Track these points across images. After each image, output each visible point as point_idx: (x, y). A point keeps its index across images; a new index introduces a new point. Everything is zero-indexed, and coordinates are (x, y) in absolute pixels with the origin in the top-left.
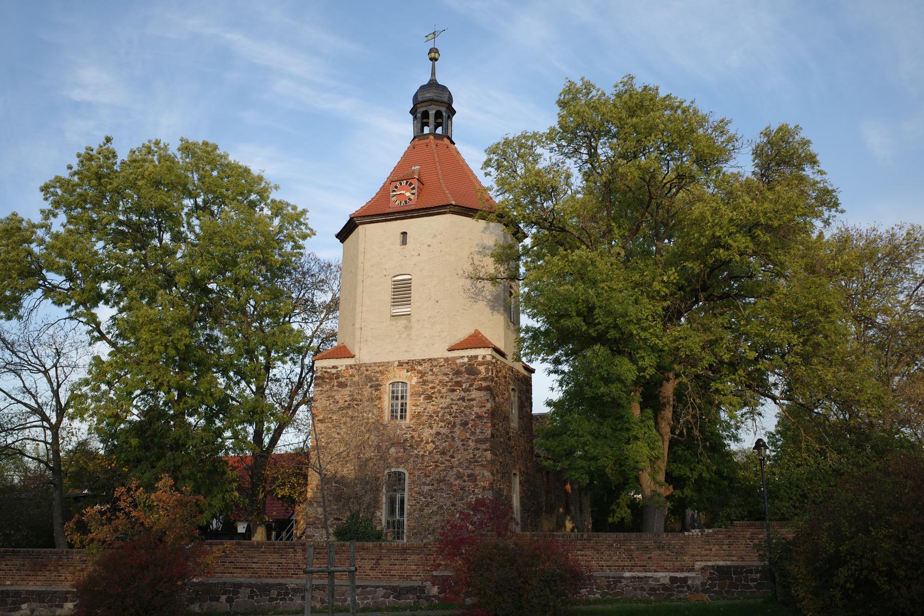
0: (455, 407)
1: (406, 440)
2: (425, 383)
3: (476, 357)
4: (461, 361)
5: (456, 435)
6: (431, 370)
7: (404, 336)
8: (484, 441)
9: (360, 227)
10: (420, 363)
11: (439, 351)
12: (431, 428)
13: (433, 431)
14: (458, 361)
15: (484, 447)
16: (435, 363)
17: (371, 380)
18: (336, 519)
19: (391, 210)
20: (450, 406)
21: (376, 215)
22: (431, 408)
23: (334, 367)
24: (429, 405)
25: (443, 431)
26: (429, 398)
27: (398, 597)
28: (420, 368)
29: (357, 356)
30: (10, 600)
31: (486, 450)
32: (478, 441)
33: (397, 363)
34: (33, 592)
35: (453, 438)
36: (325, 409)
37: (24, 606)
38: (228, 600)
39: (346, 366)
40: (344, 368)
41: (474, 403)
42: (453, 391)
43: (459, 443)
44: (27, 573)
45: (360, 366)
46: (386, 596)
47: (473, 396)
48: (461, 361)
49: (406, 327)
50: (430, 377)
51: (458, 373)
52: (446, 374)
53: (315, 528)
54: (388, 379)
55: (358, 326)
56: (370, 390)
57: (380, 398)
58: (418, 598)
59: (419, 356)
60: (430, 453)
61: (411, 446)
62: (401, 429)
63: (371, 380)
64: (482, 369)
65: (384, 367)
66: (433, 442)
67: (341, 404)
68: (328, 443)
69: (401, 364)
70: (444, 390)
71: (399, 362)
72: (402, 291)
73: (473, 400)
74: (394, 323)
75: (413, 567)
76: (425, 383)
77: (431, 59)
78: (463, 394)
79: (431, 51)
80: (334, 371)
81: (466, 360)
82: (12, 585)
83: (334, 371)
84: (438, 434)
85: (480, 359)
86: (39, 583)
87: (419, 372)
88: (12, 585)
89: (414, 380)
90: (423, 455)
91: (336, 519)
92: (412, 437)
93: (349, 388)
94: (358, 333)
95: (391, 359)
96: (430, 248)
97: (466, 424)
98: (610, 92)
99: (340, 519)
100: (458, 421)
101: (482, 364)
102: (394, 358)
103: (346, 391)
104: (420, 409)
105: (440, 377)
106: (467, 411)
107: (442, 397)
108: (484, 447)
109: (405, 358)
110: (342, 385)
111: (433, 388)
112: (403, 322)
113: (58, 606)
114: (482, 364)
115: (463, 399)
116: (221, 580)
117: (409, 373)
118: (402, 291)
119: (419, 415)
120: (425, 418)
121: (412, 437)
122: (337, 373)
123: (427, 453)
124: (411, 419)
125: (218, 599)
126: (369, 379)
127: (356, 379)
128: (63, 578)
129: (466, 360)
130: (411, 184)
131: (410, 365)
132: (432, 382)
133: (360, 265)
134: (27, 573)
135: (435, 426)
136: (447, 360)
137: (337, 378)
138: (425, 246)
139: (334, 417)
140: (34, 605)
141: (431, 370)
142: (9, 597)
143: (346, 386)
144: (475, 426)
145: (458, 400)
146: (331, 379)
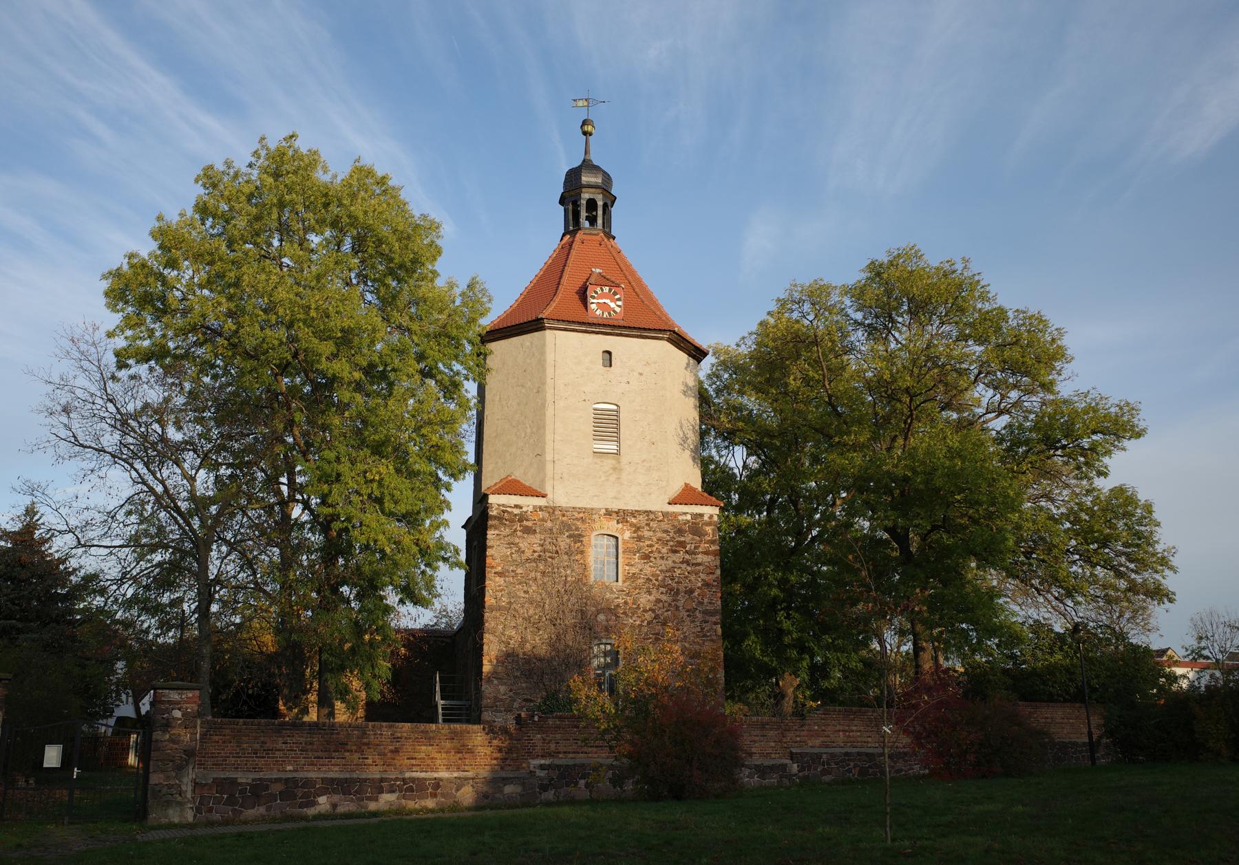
0: (678, 571)
1: (618, 606)
2: (640, 539)
3: (701, 515)
4: (684, 517)
5: (680, 604)
6: (648, 525)
7: (612, 478)
8: (712, 614)
9: (548, 332)
10: (634, 514)
11: (658, 503)
12: (650, 594)
13: (652, 598)
14: (680, 518)
15: (714, 619)
16: (652, 516)
17: (569, 529)
18: (526, 700)
19: (590, 321)
20: (672, 570)
21: (604, 325)
22: (648, 570)
23: (516, 506)
24: (647, 567)
25: (664, 598)
26: (646, 557)
27: (762, 777)
28: (633, 520)
29: (550, 496)
30: (299, 792)
31: (715, 624)
32: (705, 612)
33: (603, 511)
34: (332, 780)
35: (677, 608)
36: (504, 558)
37: (322, 800)
38: (587, 785)
39: (534, 507)
40: (531, 509)
41: (701, 568)
42: (676, 552)
43: (684, 614)
44: (316, 754)
45: (554, 509)
46: (750, 776)
47: (699, 560)
48: (684, 517)
49: (614, 469)
50: (647, 534)
51: (680, 532)
52: (666, 531)
53: (496, 711)
54: (592, 530)
55: (549, 457)
56: (568, 541)
57: (582, 552)
58: (781, 777)
59: (631, 507)
60: (649, 623)
61: (624, 613)
62: (612, 592)
63: (569, 529)
64: (709, 529)
65: (586, 515)
66: (653, 611)
67: (528, 554)
68: (510, 603)
69: (609, 513)
70: (664, 551)
71: (607, 510)
72: (608, 424)
73: (699, 564)
74: (598, 461)
75: (773, 744)
76: (640, 539)
77: (585, 133)
78: (687, 557)
79: (585, 123)
80: (516, 511)
81: (689, 517)
82: (295, 771)
83: (516, 511)
84: (658, 601)
85: (706, 518)
86: (337, 768)
87: (632, 525)
88: (295, 771)
89: (627, 535)
90: (640, 626)
91: (526, 700)
92: (626, 603)
93: (538, 536)
94: (549, 466)
95: (595, 504)
96: (642, 378)
97: (691, 591)
98: (935, 263)
99: (531, 701)
100: (682, 588)
101: (709, 524)
102: (599, 504)
103: (536, 539)
104: (634, 570)
105: (659, 535)
106: (693, 578)
107: (662, 558)
108: (714, 619)
109: (615, 506)
110: (528, 531)
111: (651, 546)
112: (610, 462)
113: (370, 799)
114: (709, 524)
115: (687, 562)
116: (578, 761)
117: (620, 526)
118: (608, 424)
119: (634, 577)
120: (641, 581)
121: (626, 603)
122: (521, 514)
123: (645, 623)
124: (624, 582)
125: (576, 783)
126: (566, 526)
127: (549, 524)
128: (370, 761)
129: (689, 517)
130: (615, 294)
131: (622, 516)
132: (650, 539)
133: (549, 381)
134: (316, 754)
135: (654, 591)
136: (665, 514)
137: (520, 521)
138: (636, 374)
139: (519, 571)
140: (336, 798)
141: (648, 525)
142: (297, 787)
143: (535, 532)
144: (703, 595)
145: (682, 563)
146: (512, 521)
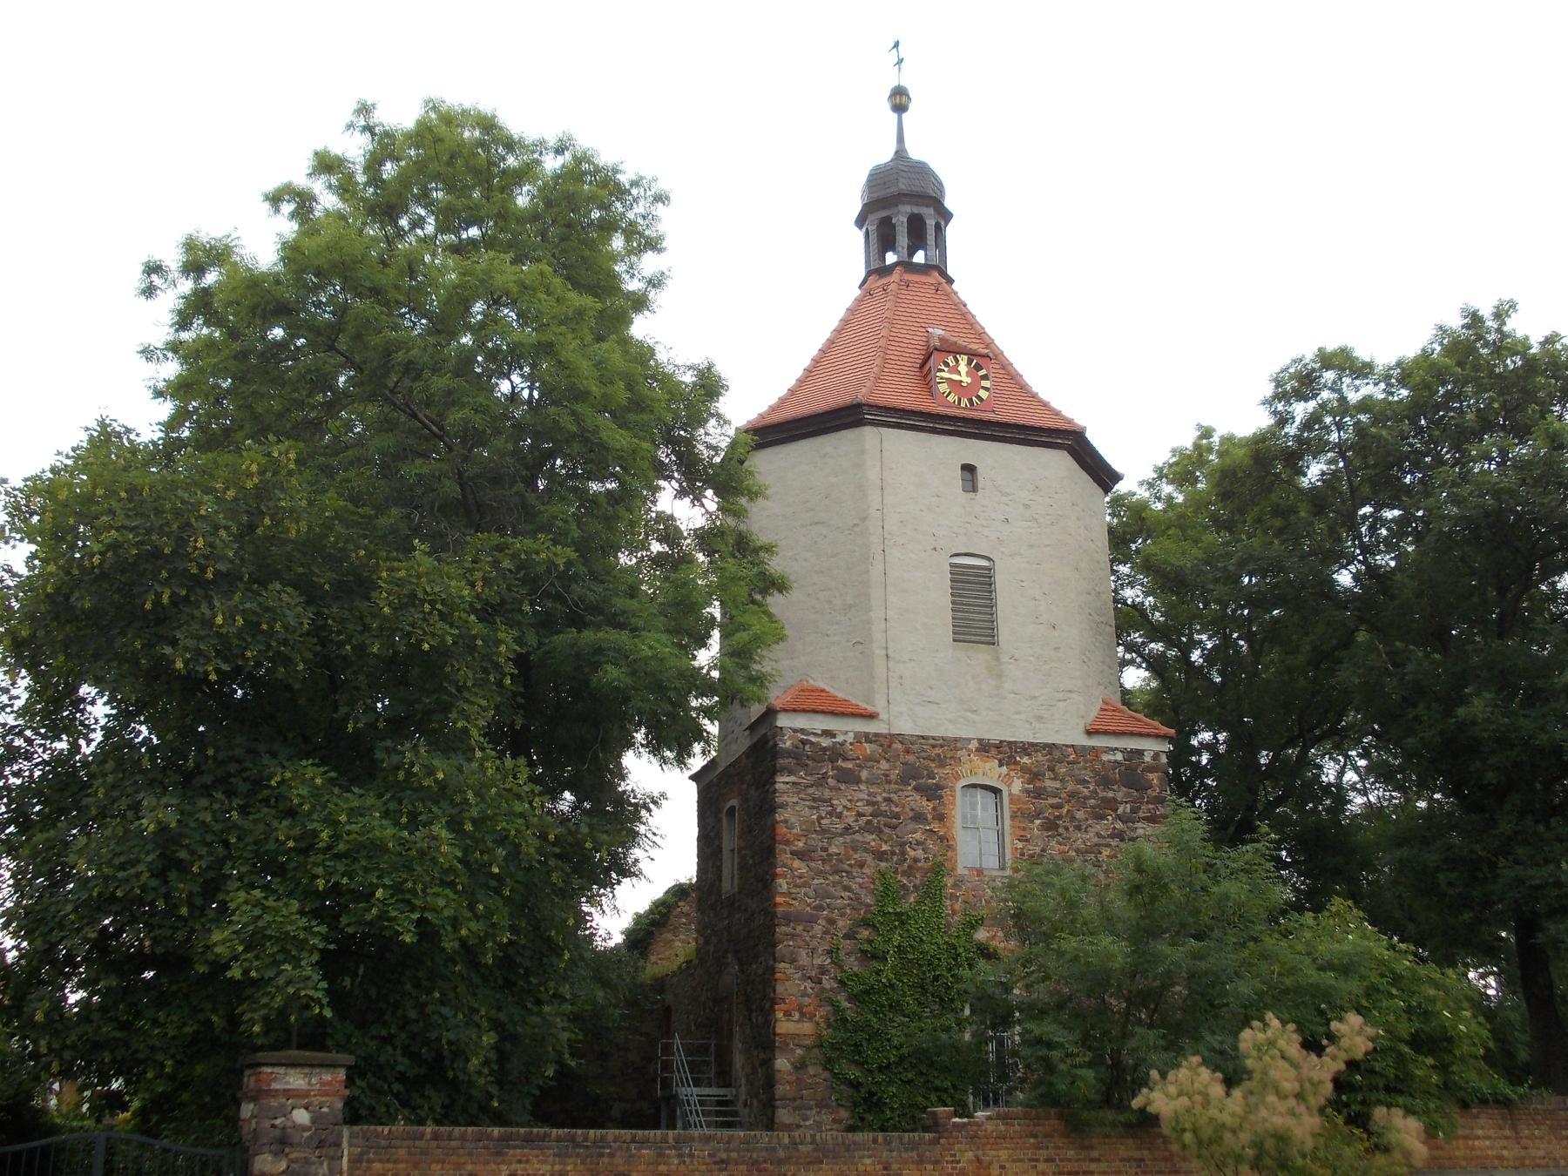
3: (1140, 753)
6: (1051, 769)
9: (868, 431)
10: (1028, 748)
16: (1057, 754)
23: (828, 733)
28: (1026, 760)
29: (884, 716)
33: (974, 745)
39: (857, 734)
40: (850, 738)
45: (892, 738)
50: (1049, 784)
54: (957, 777)
59: (1024, 735)
64: (1154, 778)
65: (945, 750)
69: (985, 747)
71: (980, 741)
76: (1038, 794)
78: (1119, 825)
80: (826, 742)
81: (1119, 757)
85: (1148, 758)
87: (1024, 769)
89: (1017, 786)
103: (862, 793)
105: (1071, 786)
107: (1078, 828)
109: (995, 735)
111: (1058, 807)
115: (1120, 835)
122: (832, 748)
131: (1007, 752)
136: (1081, 751)
143: (858, 781)
145: (1112, 836)
